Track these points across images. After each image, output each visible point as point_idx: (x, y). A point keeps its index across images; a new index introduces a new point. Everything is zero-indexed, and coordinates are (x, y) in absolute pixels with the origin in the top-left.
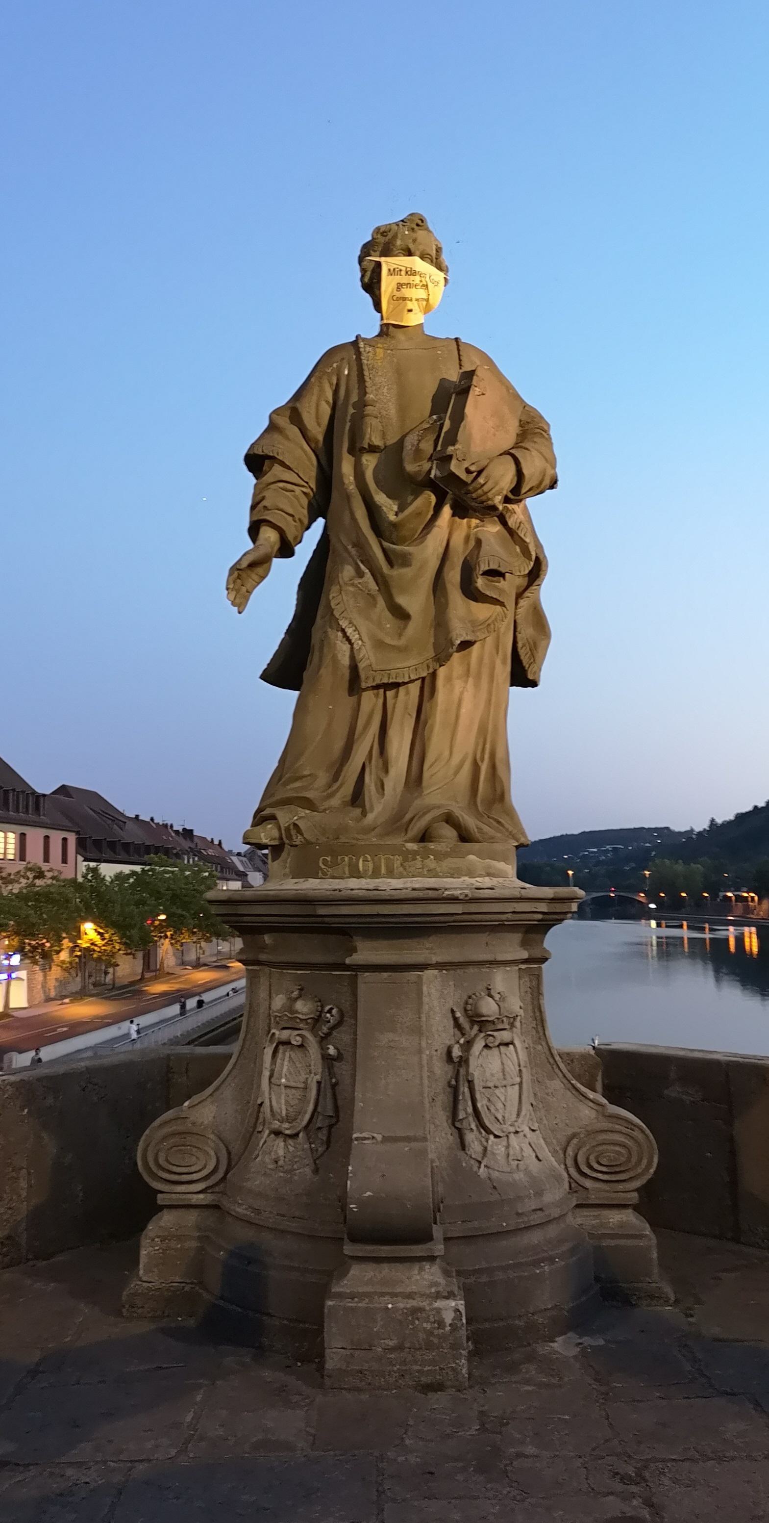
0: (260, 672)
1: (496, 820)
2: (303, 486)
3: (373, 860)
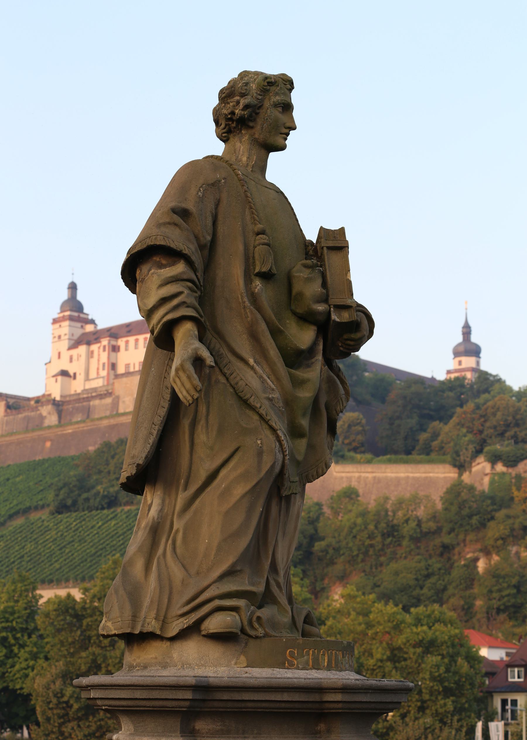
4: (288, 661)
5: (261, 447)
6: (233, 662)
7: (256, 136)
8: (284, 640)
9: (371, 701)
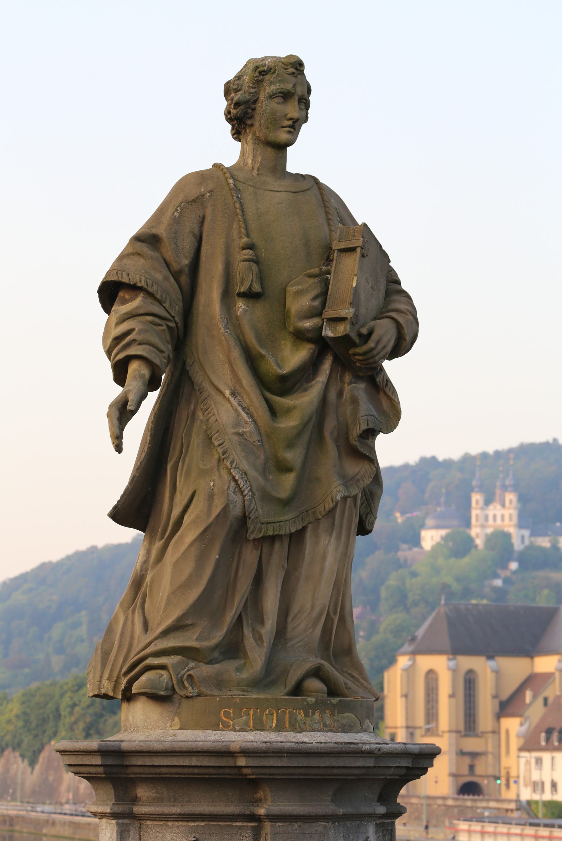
0: (110, 508)
1: (350, 674)
2: (170, 320)
3: (277, 714)
4: (223, 722)
5: (212, 489)
6: (168, 725)
7: (257, 134)
8: (218, 699)
9: (290, 765)
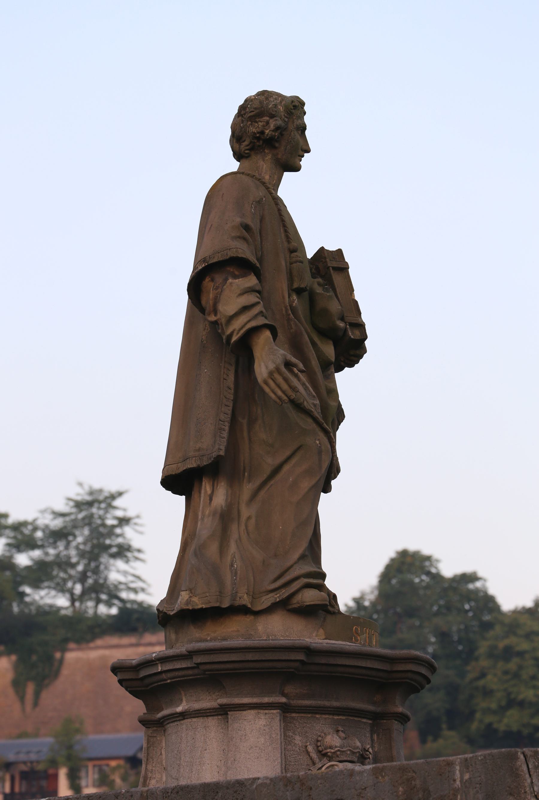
5: (320, 447)
6: (314, 634)
7: (279, 157)
